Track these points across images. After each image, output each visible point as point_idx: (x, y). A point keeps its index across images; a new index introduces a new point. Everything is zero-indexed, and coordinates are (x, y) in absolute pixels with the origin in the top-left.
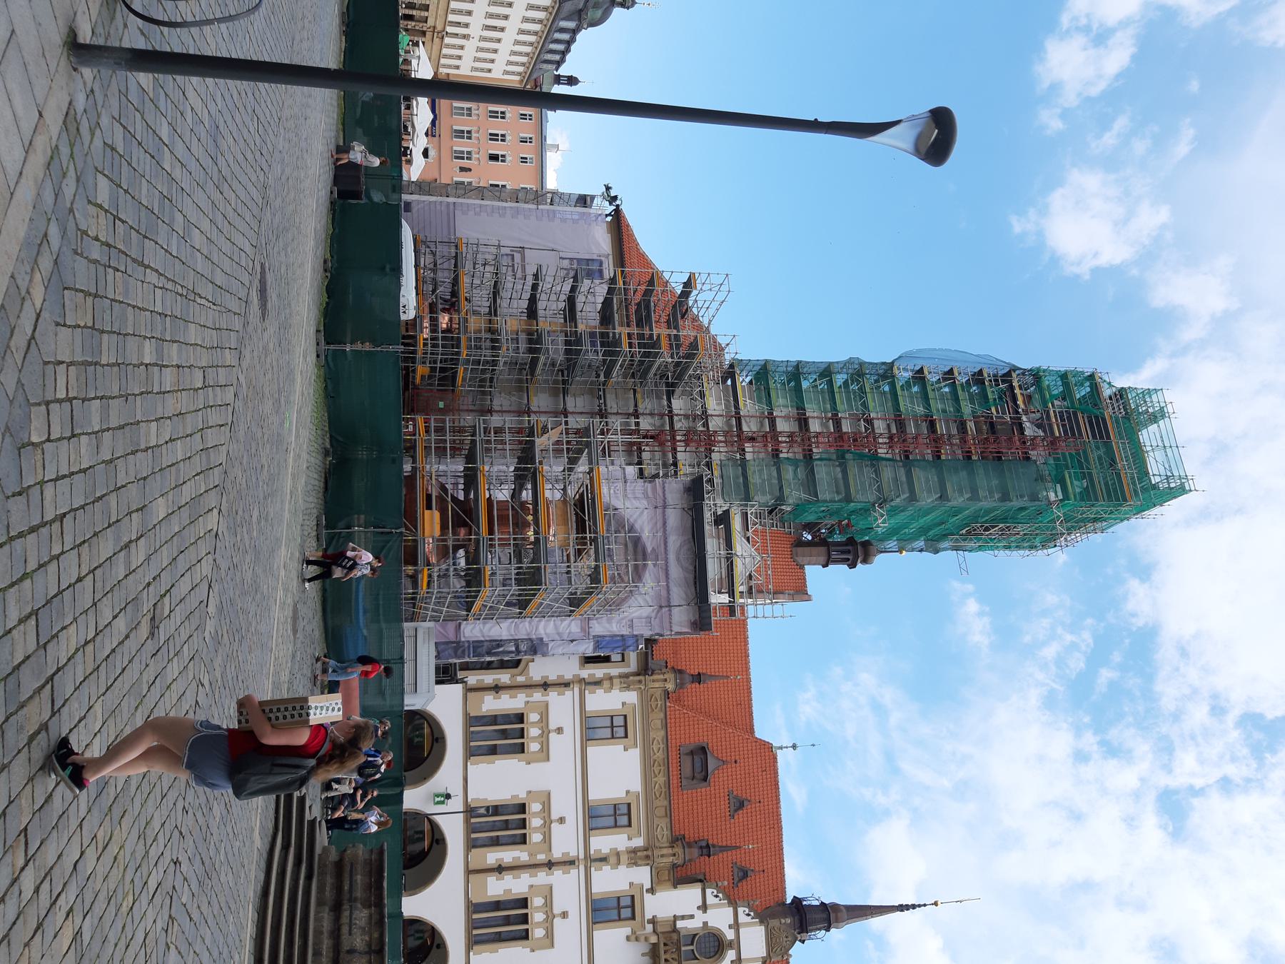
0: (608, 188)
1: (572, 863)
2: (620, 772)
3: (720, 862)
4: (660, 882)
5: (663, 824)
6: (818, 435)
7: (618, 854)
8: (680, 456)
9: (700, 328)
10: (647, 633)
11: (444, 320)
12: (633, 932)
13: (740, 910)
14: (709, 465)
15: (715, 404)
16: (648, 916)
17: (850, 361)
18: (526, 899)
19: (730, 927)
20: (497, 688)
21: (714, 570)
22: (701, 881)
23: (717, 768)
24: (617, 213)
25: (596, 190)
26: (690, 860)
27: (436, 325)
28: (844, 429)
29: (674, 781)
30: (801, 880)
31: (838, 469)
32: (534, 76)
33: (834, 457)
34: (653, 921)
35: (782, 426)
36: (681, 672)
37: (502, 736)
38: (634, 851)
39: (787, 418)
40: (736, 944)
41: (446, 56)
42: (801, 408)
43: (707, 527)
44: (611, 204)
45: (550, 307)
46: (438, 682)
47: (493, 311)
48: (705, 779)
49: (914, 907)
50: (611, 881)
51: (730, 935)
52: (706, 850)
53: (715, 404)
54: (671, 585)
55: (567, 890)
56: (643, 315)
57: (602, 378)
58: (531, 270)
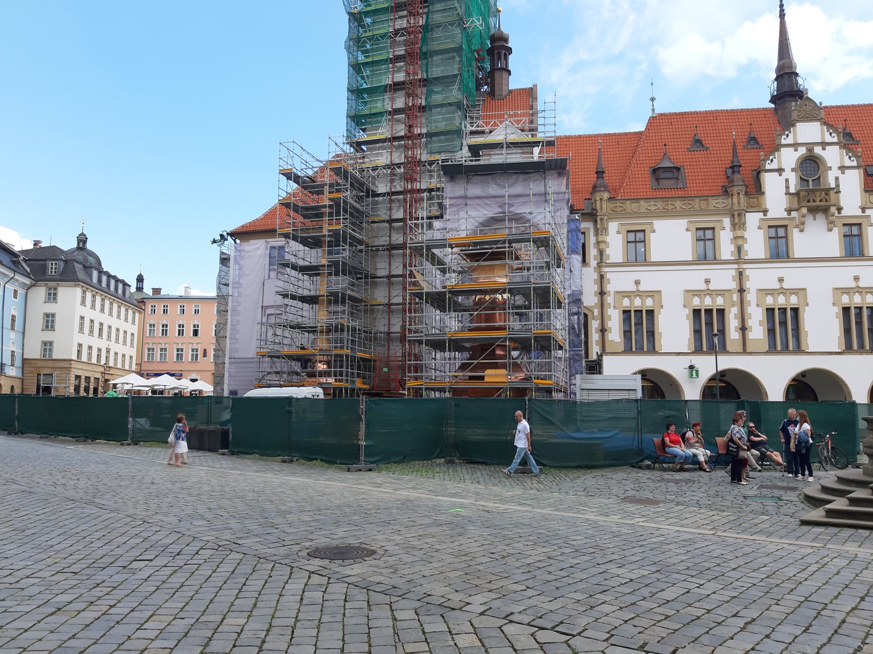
0: (214, 241)
1: (741, 274)
2: (671, 236)
3: (746, 157)
4: (759, 205)
5: (713, 202)
6: (408, 73)
7: (736, 238)
8: (424, 187)
9: (322, 169)
10: (566, 212)
11: (322, 367)
12: (797, 226)
13: (783, 142)
14: (431, 163)
15: (383, 159)
17: (348, 48)
18: (767, 309)
19: (796, 150)
20: (603, 330)
21: (516, 157)
22: (758, 173)
23: (670, 159)
24: (234, 234)
25: (216, 250)
26: (743, 181)
27: (325, 372)
28: (402, 53)
29: (679, 193)
30: (760, 96)
31: (434, 58)
32: (135, 302)
33: (425, 61)
34: (789, 211)
35: (400, 103)
36: (595, 187)
37: (641, 328)
38: (734, 226)
39: (393, 100)
40: (810, 146)
41: (123, 365)
42: (385, 89)
43: (481, 163)
44: (226, 240)
45: (306, 285)
46: (600, 373)
47: (313, 330)
48: (678, 169)
50: (756, 243)
51: (802, 151)
52: (735, 168)
53: (383, 159)
54: (527, 192)
55: (761, 278)
56: (312, 213)
57: (363, 247)
58: (280, 300)
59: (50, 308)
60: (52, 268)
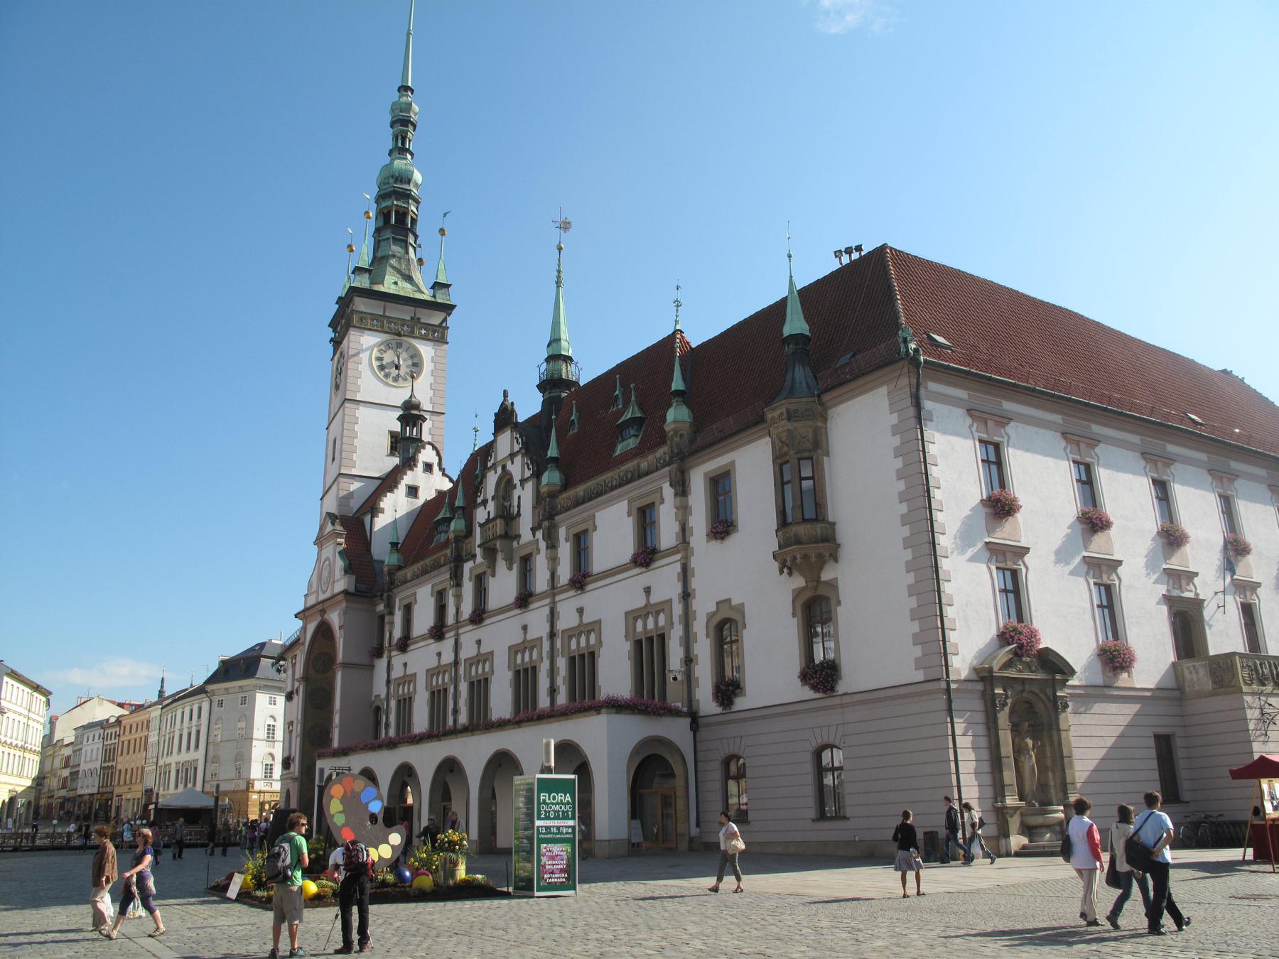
20: (387, 725)
49: (559, 271)
51: (499, 470)
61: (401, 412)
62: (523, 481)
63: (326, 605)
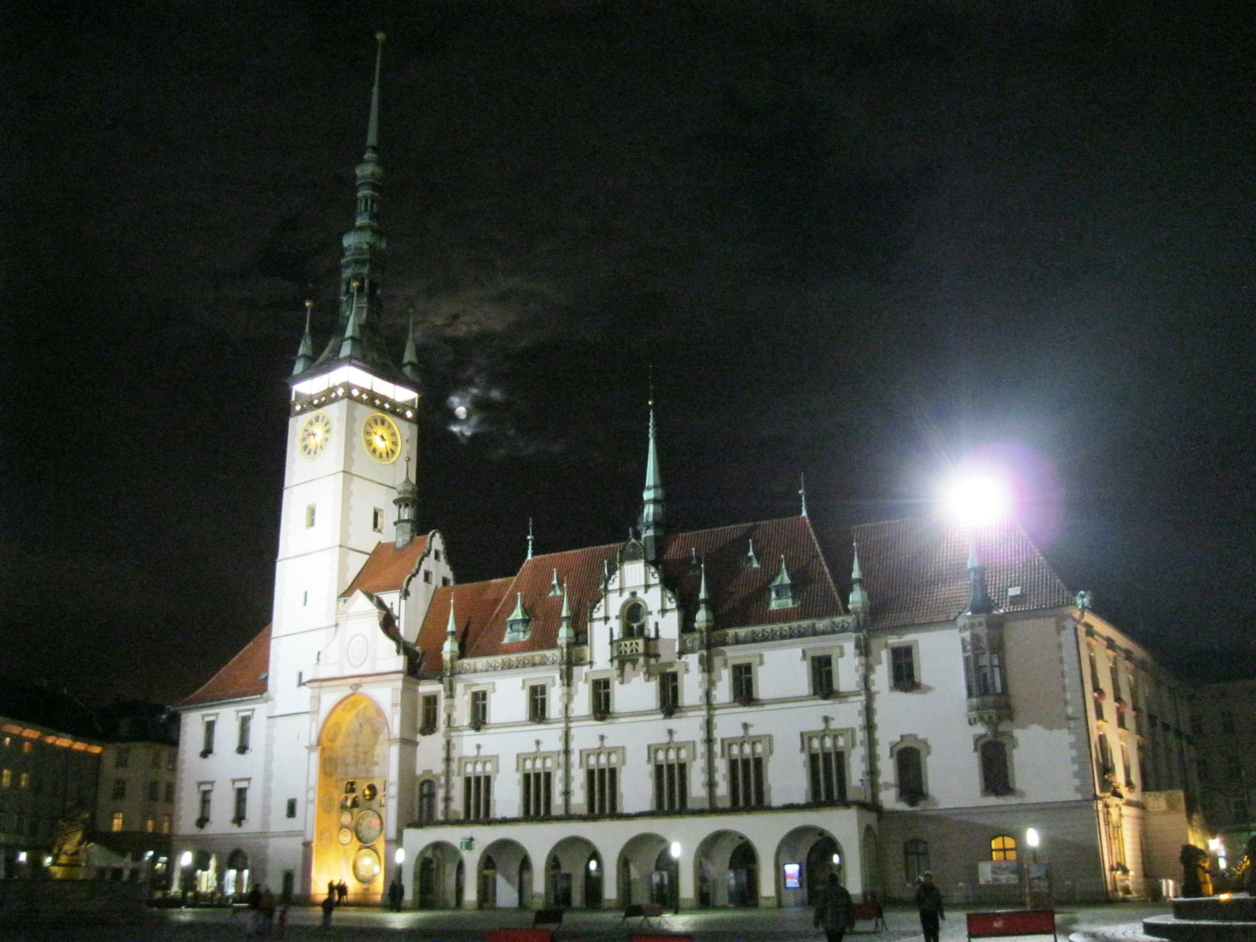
16: (608, 665)
20: (447, 799)
34: (611, 660)
50: (583, 701)
51: (626, 595)
59: (122, 773)
60: (124, 726)
61: (396, 496)
62: (664, 611)
63: (364, 680)
